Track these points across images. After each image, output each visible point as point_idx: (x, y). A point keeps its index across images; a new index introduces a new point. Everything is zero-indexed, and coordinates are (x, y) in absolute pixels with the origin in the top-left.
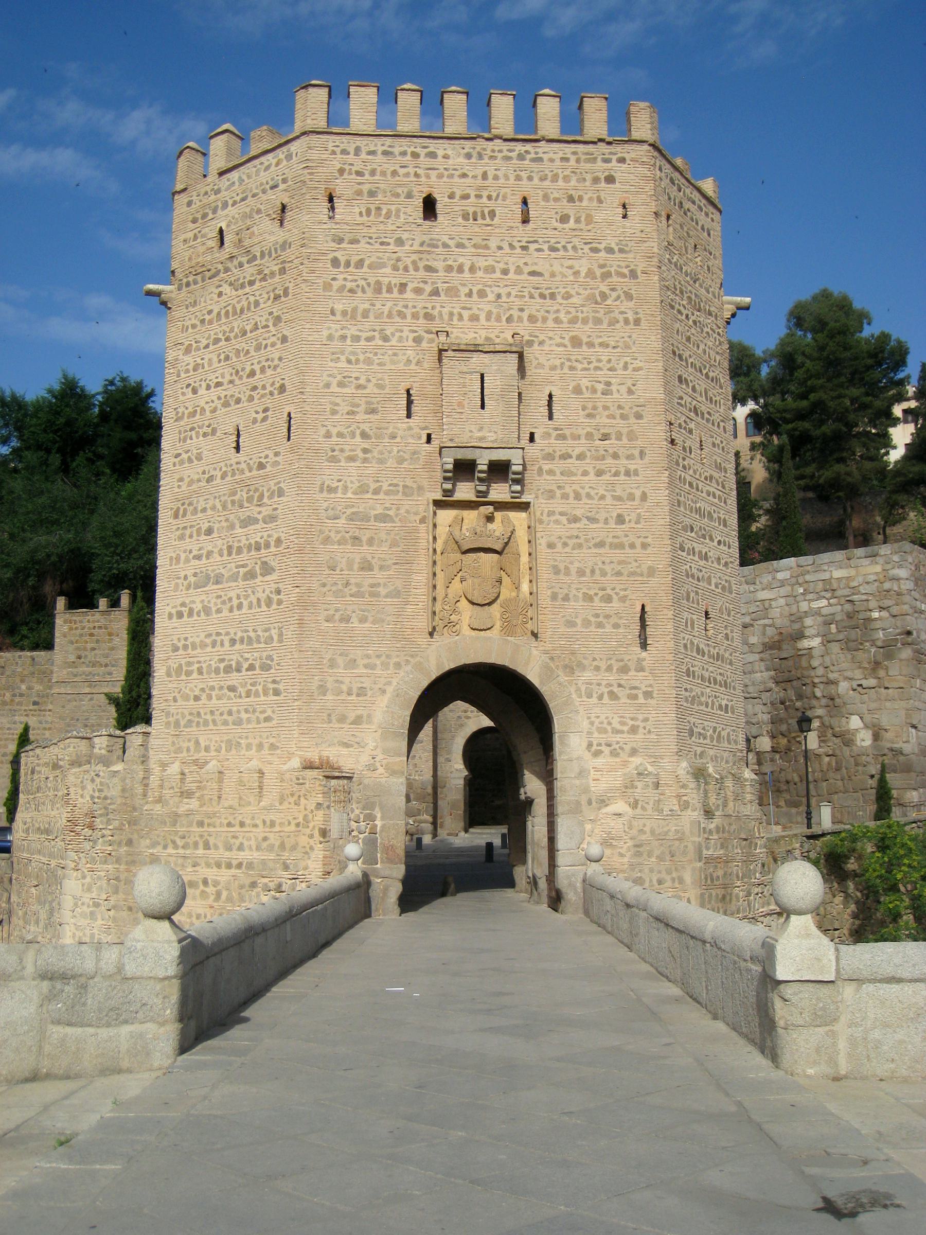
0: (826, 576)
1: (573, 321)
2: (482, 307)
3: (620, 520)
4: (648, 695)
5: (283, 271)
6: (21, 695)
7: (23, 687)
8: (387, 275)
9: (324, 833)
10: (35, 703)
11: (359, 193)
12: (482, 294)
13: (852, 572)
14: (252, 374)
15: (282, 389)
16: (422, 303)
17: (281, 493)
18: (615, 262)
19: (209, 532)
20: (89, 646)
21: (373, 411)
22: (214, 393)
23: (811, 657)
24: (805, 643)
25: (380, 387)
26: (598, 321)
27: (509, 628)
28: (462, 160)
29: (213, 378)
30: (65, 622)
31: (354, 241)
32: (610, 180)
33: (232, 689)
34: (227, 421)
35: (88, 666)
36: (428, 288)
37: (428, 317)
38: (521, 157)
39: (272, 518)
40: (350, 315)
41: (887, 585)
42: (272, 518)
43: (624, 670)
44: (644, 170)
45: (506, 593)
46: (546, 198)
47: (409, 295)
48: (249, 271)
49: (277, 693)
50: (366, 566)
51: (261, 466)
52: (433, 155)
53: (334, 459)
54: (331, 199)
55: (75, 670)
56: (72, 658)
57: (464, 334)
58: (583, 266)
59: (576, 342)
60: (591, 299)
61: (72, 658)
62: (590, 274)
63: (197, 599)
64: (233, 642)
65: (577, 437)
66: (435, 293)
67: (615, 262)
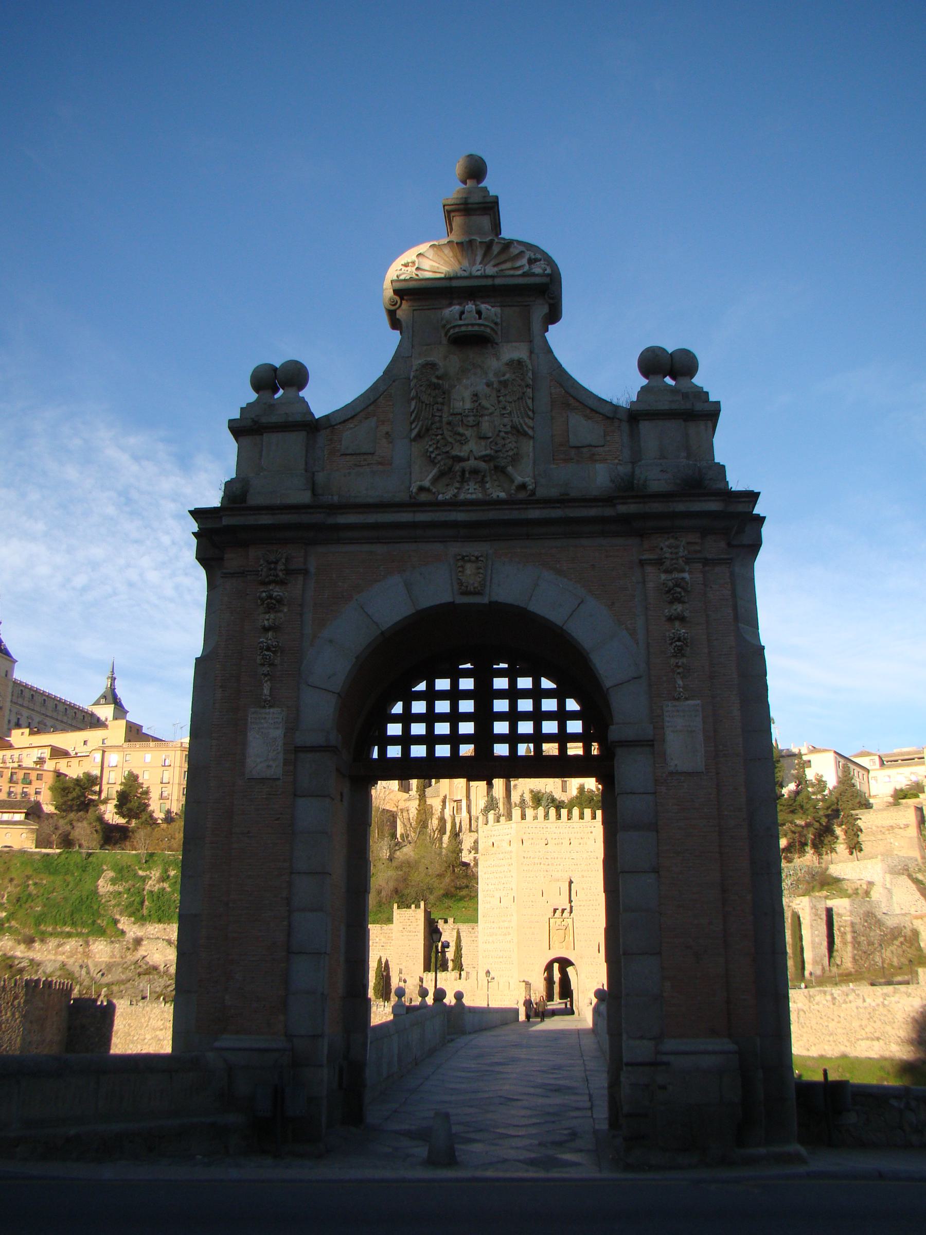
6: (376, 943)
7: (377, 939)
8: (536, 860)
15: (512, 889)
20: (408, 924)
22: (493, 886)
27: (567, 949)
28: (554, 829)
32: (591, 832)
36: (547, 863)
37: (547, 871)
39: (510, 921)
42: (510, 921)
47: (542, 865)
48: (501, 856)
49: (513, 964)
50: (533, 934)
52: (547, 828)
53: (525, 908)
59: (583, 877)
60: (586, 865)
62: (586, 858)
66: (549, 865)
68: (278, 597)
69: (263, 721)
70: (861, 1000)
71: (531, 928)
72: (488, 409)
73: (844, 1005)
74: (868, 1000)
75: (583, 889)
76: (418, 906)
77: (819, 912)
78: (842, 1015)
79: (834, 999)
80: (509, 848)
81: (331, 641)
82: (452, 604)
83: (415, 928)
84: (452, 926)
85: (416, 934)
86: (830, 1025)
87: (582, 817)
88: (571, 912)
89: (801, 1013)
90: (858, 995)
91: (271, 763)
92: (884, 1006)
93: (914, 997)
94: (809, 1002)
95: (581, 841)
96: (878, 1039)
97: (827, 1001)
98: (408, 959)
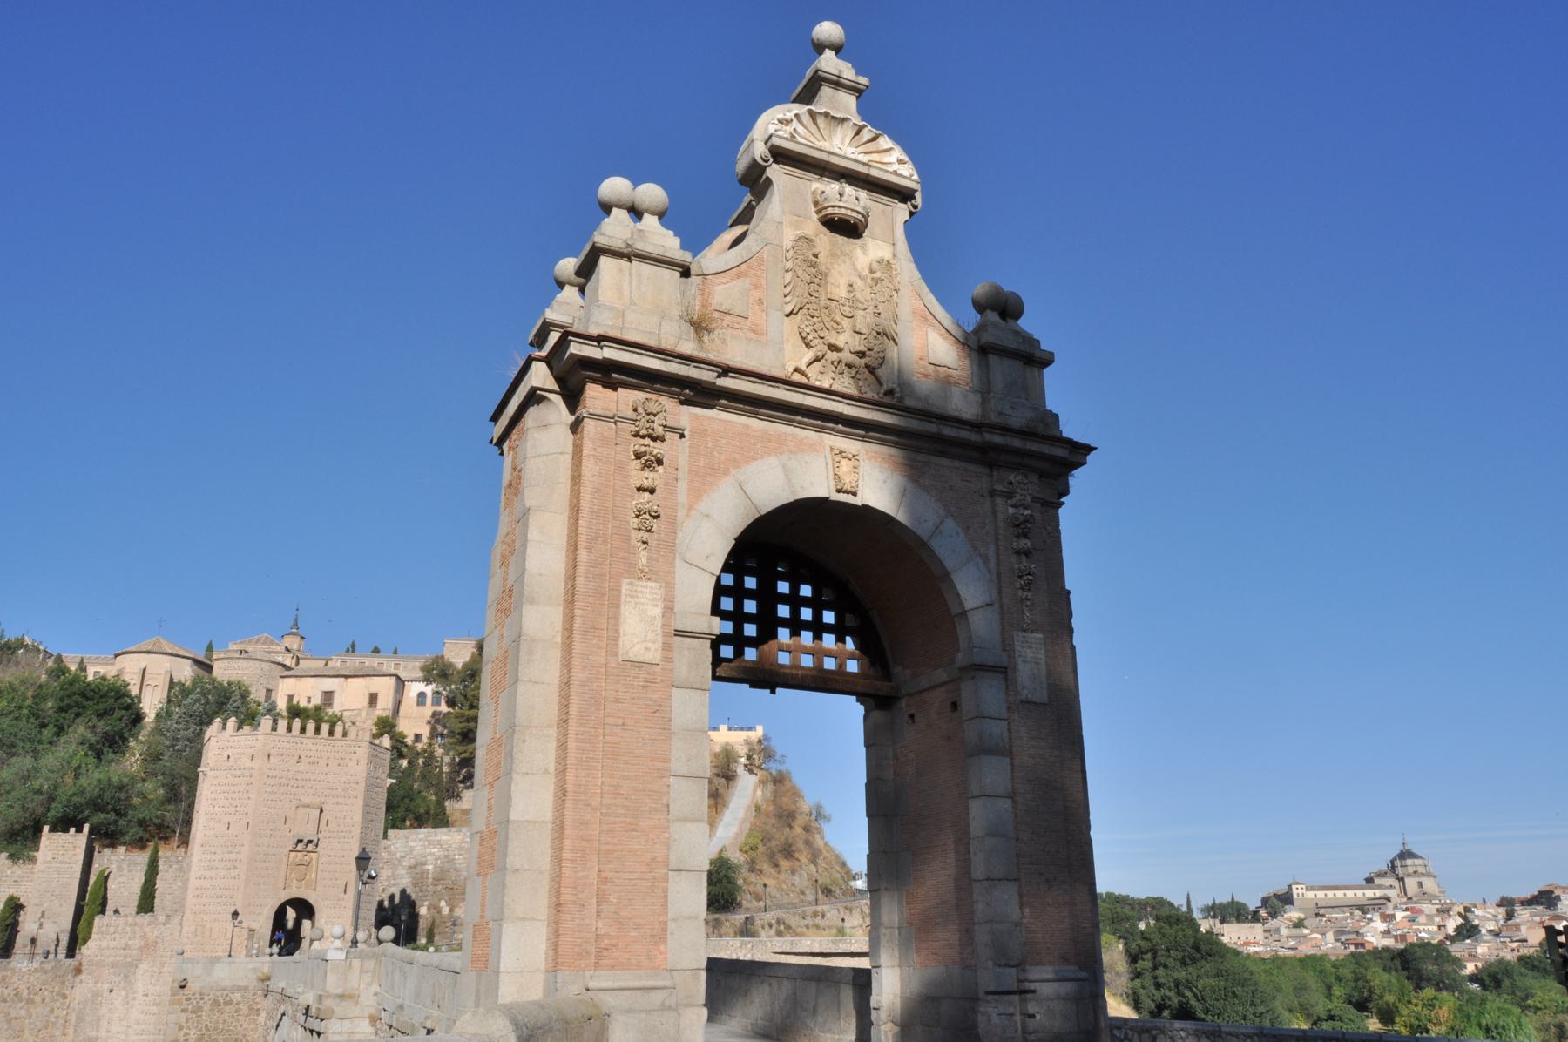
0: (439, 838)
1: (337, 797)
3: (343, 856)
4: (345, 907)
5: (251, 776)
6: (7, 876)
8: (284, 781)
9: (246, 947)
10: (15, 881)
11: (278, 755)
12: (312, 788)
13: (449, 838)
14: (236, 806)
15: (247, 814)
16: (294, 790)
17: (243, 845)
19: (215, 853)
20: (61, 852)
21: (274, 823)
22: (221, 809)
23: (428, 873)
24: (427, 867)
25: (277, 815)
26: (345, 797)
29: (221, 804)
30: (48, 839)
31: (275, 770)
32: (355, 753)
33: (218, 903)
34: (226, 819)
35: (58, 863)
38: (329, 745)
40: (271, 793)
41: (463, 845)
43: (339, 900)
44: (364, 750)
45: (308, 877)
46: (335, 758)
47: (289, 787)
48: (238, 773)
50: (267, 869)
51: (237, 836)
52: (302, 743)
54: (269, 756)
55: (49, 865)
56: (50, 859)
57: (306, 800)
58: (343, 780)
59: (338, 803)
60: (344, 790)
61: (50, 859)
62: (345, 783)
63: (208, 874)
64: (220, 889)
65: (333, 832)
68: (659, 455)
69: (639, 595)
71: (265, 861)
72: (863, 304)
75: (336, 818)
76: (79, 830)
80: (248, 764)
81: (707, 516)
82: (825, 500)
83: (71, 858)
84: (122, 857)
85: (72, 865)
87: (303, 730)
91: (649, 645)
98: (53, 898)
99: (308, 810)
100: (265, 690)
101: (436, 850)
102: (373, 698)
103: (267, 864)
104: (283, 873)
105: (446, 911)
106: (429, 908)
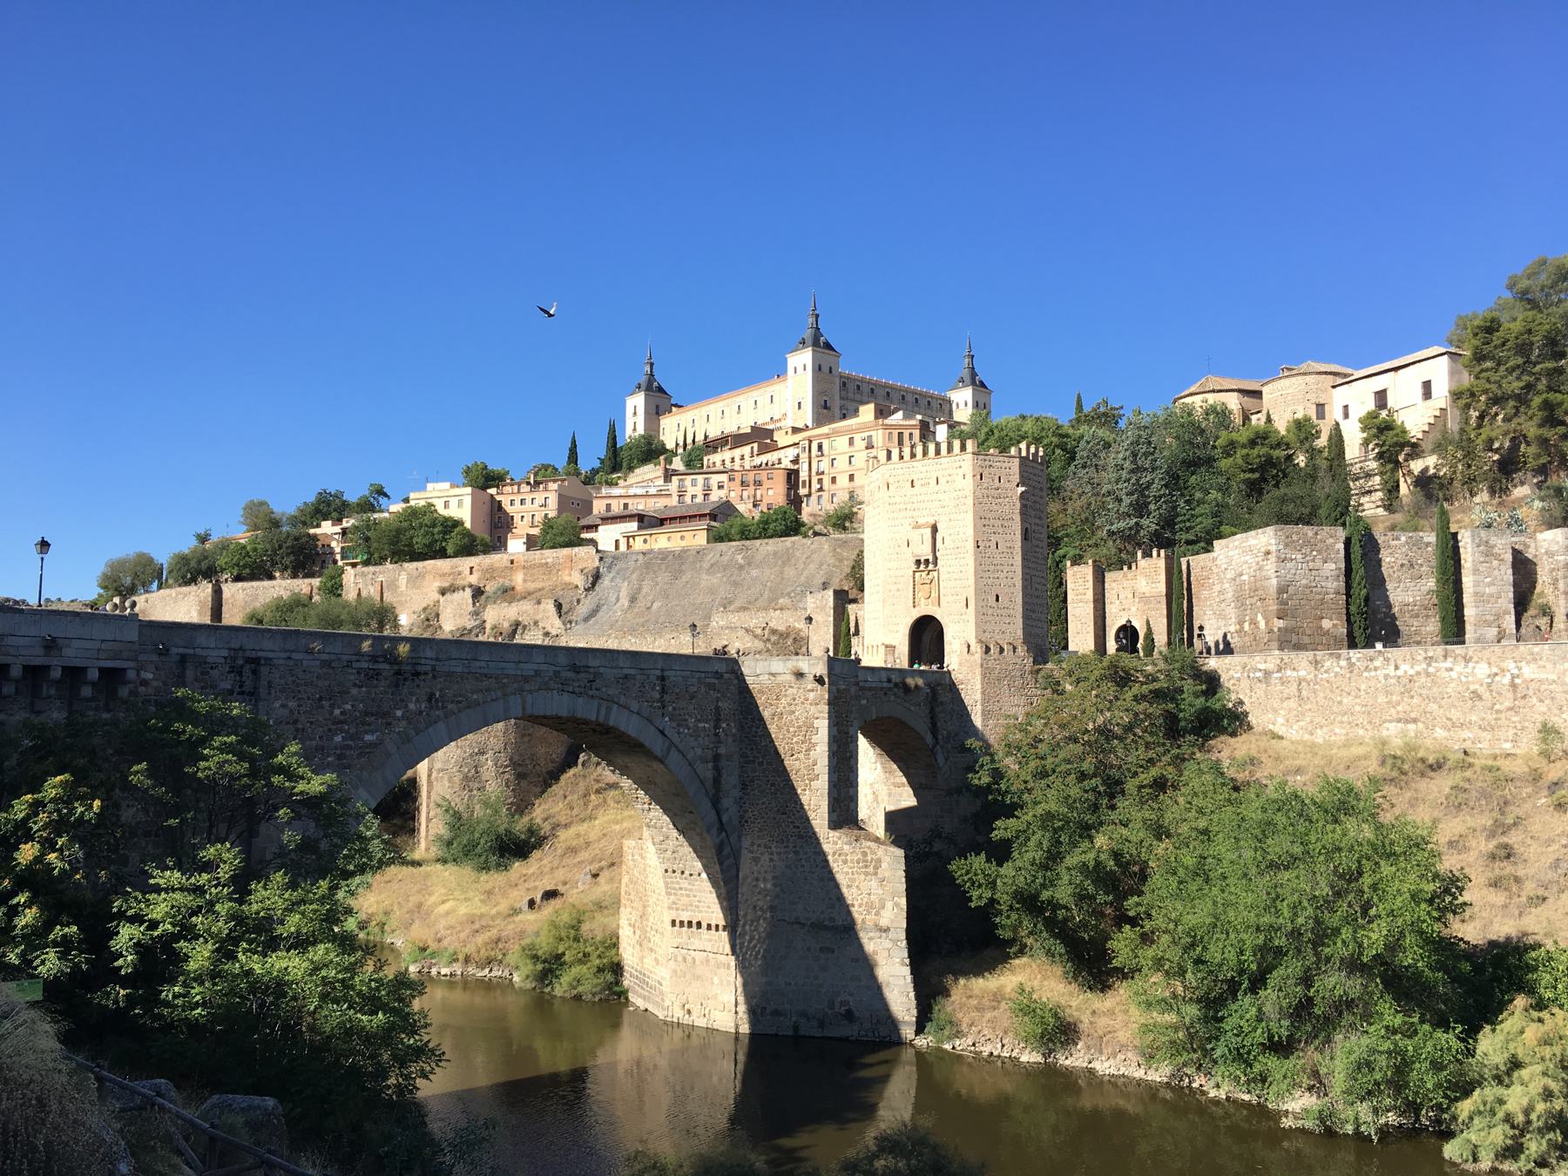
2: (925, 513)
18: (960, 494)
50: (898, 590)
57: (921, 521)
67: (960, 494)
70: (1392, 667)
73: (1366, 674)
74: (1404, 667)
77: (1496, 550)
78: (1363, 687)
79: (1351, 665)
86: (1345, 701)
88: (935, 564)
89: (1303, 684)
90: (1387, 660)
92: (1428, 675)
93: (1477, 662)
94: (1316, 668)
95: (949, 478)
96: (1415, 721)
97: (1341, 668)
99: (922, 531)
100: (1314, 406)
101: (1248, 557)
102: (1427, 386)
103: (898, 586)
104: (912, 593)
105: (1262, 624)
106: (1250, 624)
